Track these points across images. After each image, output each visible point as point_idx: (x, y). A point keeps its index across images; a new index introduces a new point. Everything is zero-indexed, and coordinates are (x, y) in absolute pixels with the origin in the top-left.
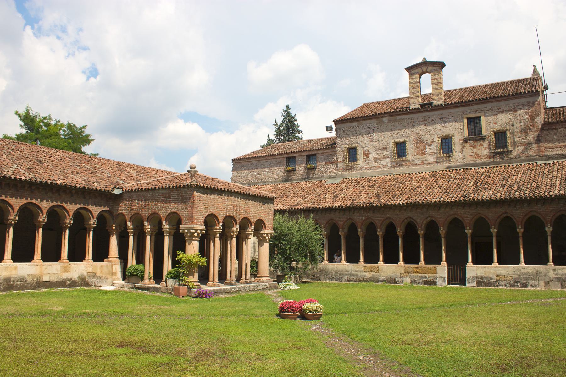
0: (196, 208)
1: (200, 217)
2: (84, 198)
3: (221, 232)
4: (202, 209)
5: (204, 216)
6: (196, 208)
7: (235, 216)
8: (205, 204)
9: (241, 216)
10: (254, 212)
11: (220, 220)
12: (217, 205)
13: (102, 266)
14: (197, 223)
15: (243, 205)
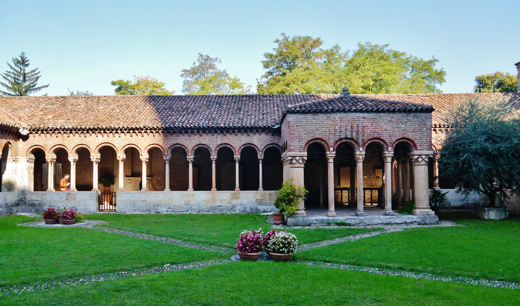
0: (293, 134)
1: (298, 144)
2: (248, 135)
3: (335, 156)
4: (300, 134)
5: (304, 142)
6: (293, 134)
7: (355, 138)
8: (306, 129)
9: (366, 137)
10: (391, 130)
11: (330, 145)
12: (324, 129)
13: (270, 194)
14: (295, 149)
15: (369, 125)
